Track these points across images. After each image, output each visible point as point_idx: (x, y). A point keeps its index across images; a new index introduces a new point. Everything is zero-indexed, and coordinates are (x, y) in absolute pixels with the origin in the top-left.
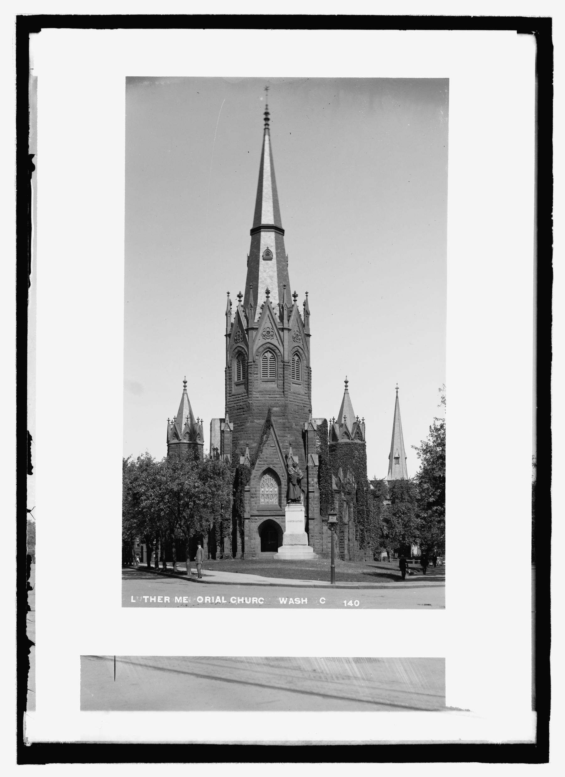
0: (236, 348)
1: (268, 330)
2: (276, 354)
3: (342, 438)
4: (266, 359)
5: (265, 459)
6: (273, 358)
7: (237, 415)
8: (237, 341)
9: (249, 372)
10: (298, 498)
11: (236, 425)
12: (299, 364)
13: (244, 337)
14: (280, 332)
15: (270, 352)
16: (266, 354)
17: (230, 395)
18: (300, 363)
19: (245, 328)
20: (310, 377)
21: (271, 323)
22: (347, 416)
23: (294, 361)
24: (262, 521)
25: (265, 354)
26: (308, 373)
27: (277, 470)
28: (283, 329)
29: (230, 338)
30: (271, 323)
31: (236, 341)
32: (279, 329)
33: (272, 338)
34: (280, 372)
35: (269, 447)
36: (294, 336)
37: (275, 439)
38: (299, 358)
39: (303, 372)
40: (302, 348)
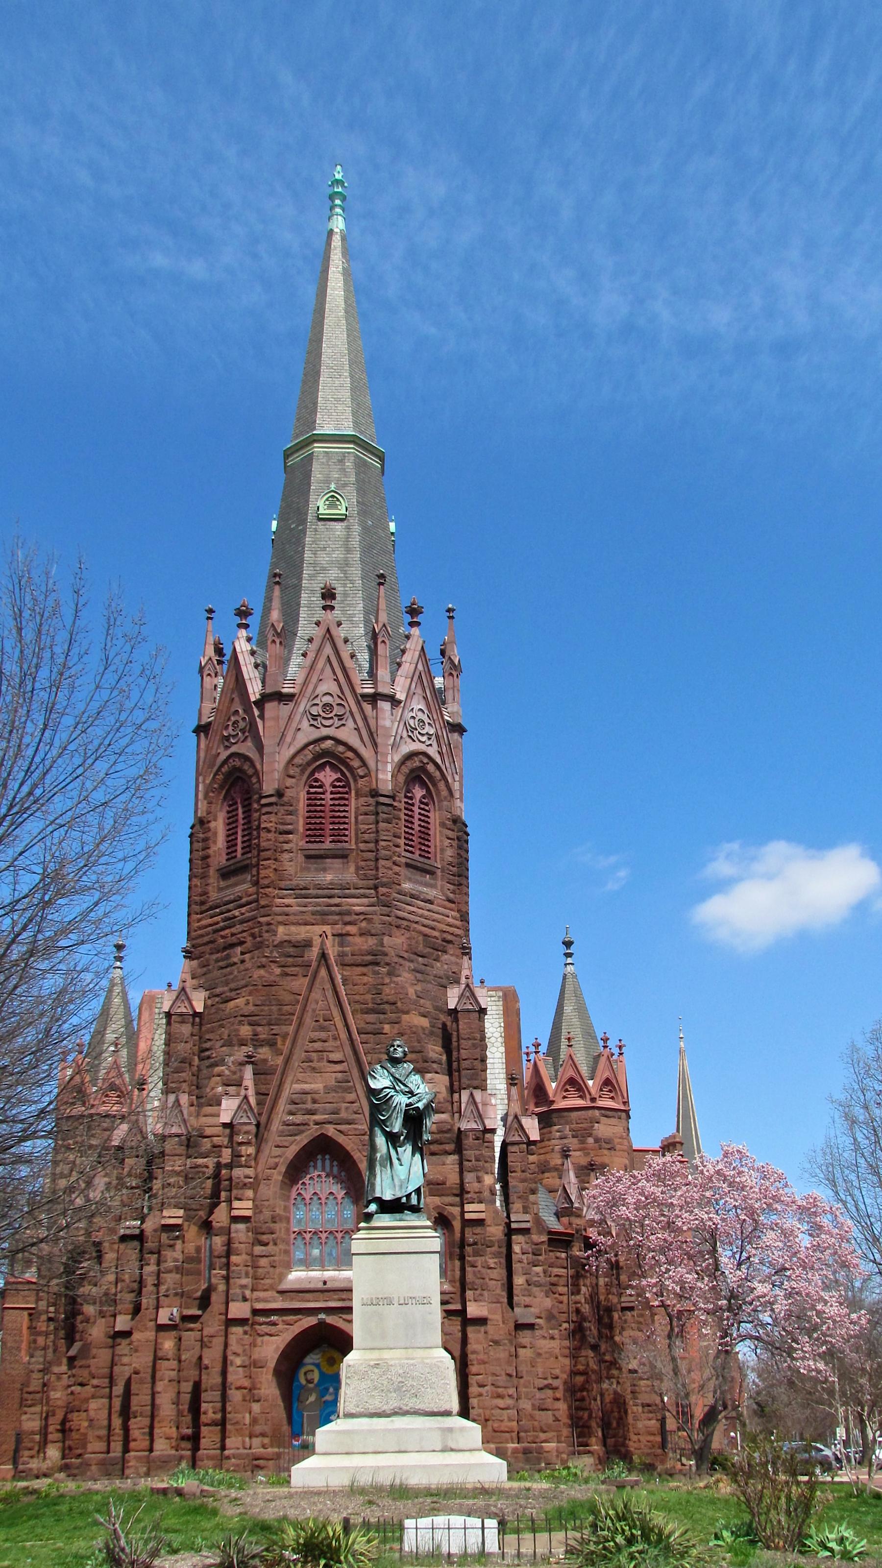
0: (225, 762)
1: (327, 699)
2: (352, 773)
3: (565, 1097)
4: (320, 787)
5: (309, 1106)
6: (343, 787)
7: (222, 968)
8: (228, 740)
9: (263, 826)
10: (408, 1196)
11: (217, 999)
12: (428, 811)
13: (253, 725)
14: (367, 708)
15: (334, 768)
16: (320, 776)
17: (204, 908)
18: (431, 806)
19: (253, 699)
20: (464, 881)
21: (337, 680)
22: (577, 1033)
23: (411, 798)
24: (296, 1329)
25: (317, 775)
26: (459, 839)
27: (349, 1143)
28: (374, 698)
29: (206, 737)
30: (337, 680)
31: (226, 743)
32: (364, 696)
33: (337, 723)
34: (363, 827)
35: (325, 1063)
36: (412, 722)
37: (344, 1036)
38: (428, 790)
39: (439, 838)
40: (439, 760)
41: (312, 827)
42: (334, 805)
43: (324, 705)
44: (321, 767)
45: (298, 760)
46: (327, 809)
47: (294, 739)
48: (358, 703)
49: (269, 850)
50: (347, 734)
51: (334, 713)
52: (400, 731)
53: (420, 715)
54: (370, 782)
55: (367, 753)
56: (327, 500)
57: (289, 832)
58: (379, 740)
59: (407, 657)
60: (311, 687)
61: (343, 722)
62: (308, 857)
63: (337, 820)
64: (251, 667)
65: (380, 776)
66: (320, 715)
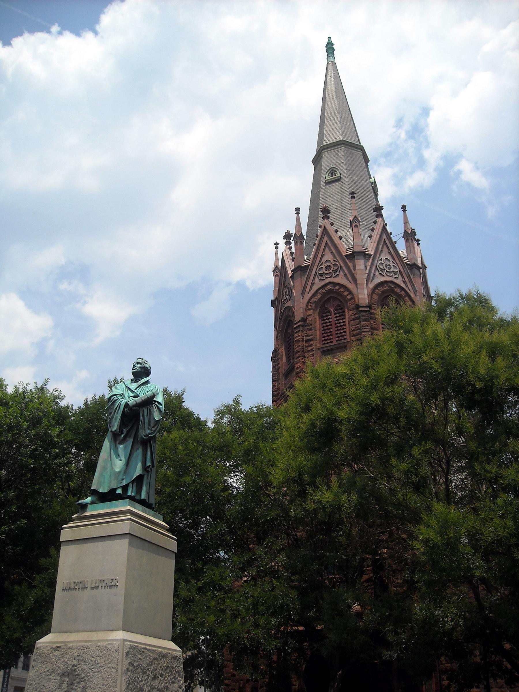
1: (328, 264)
32: (346, 256)
40: (403, 285)
41: (326, 335)
42: (337, 320)
43: (326, 267)
44: (328, 300)
45: (313, 300)
46: (333, 323)
47: (311, 289)
48: (344, 261)
49: (299, 352)
50: (341, 279)
51: (332, 269)
52: (373, 271)
53: (387, 262)
54: (355, 301)
55: (351, 286)
56: (330, 173)
57: (311, 340)
58: (358, 277)
59: (376, 232)
60: (318, 259)
61: (338, 273)
62: (322, 352)
63: (339, 328)
64: (290, 261)
65: (360, 296)
66: (324, 273)
